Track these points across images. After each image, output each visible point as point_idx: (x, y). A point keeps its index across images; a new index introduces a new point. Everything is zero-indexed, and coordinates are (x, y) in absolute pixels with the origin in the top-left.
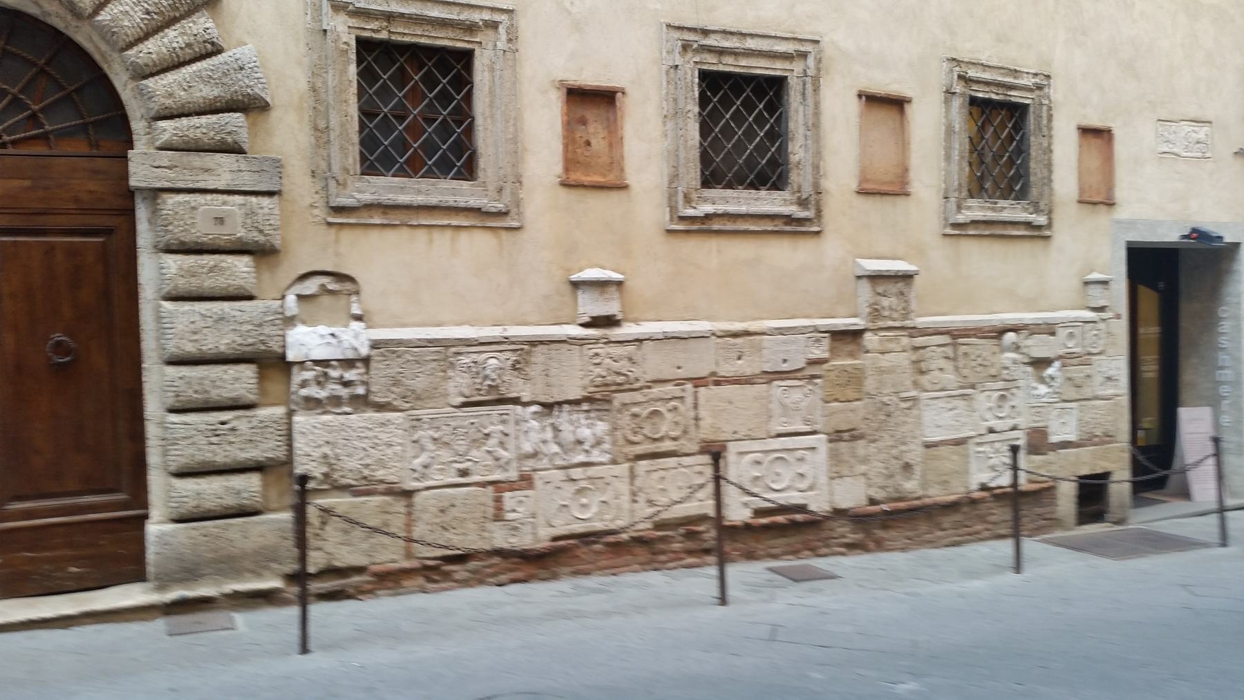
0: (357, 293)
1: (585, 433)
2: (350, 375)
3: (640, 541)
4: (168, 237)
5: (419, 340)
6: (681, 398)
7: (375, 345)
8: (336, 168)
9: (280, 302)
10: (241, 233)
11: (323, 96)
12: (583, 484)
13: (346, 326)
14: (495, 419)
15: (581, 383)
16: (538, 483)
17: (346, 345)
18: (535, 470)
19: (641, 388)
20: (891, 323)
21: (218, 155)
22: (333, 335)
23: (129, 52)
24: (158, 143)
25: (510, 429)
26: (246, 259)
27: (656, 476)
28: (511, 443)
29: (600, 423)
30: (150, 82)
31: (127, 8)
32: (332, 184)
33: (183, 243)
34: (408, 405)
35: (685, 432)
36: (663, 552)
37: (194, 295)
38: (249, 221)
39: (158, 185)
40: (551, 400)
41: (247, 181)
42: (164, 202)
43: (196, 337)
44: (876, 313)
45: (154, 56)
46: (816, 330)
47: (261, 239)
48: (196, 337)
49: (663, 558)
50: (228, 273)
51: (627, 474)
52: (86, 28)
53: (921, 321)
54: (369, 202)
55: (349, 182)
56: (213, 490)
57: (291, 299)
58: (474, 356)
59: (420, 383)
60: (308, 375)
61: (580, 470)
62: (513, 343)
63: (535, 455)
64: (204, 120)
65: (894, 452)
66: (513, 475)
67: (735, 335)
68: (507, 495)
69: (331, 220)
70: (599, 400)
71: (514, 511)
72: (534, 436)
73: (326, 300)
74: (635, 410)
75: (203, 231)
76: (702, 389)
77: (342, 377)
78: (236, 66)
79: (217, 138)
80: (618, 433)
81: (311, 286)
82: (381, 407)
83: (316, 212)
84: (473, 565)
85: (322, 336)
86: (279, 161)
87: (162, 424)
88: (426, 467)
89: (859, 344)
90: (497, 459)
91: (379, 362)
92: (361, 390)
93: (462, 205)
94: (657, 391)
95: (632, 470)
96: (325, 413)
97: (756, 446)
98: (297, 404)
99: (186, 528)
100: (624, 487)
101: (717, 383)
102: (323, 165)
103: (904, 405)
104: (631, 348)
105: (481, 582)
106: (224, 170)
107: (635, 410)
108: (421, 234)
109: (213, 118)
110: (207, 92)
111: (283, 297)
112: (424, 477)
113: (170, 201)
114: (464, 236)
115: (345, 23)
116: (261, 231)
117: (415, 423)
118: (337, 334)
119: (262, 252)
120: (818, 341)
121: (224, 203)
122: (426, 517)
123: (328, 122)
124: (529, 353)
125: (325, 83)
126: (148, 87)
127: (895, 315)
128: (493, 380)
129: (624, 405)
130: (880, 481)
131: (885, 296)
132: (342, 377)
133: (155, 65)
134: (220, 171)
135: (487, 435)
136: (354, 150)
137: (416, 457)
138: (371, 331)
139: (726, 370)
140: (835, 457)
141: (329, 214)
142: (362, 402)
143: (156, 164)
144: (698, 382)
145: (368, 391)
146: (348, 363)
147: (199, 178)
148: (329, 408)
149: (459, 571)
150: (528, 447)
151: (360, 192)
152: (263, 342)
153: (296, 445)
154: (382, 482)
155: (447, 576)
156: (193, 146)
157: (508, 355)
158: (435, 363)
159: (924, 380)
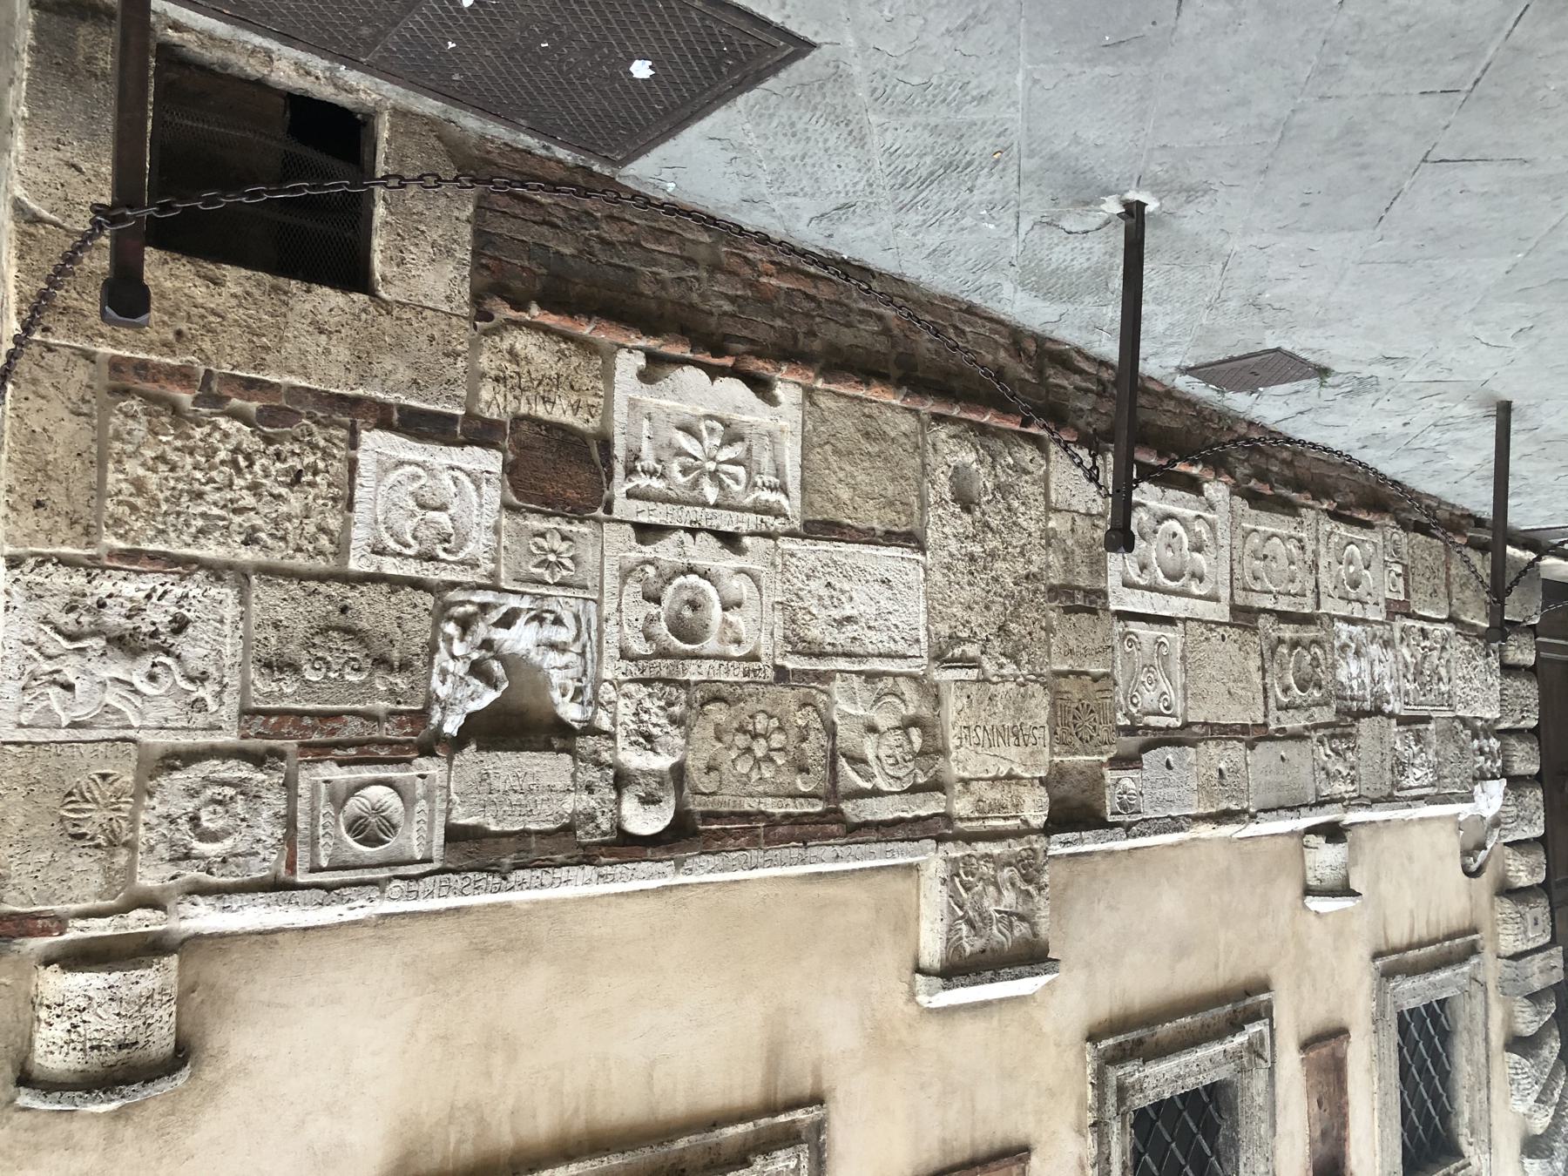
20: (996, 849)
44: (1029, 870)
65: (993, 543)
103: (972, 650)
127: (987, 869)
130: (1028, 488)
131: (1010, 914)
159: (914, 705)
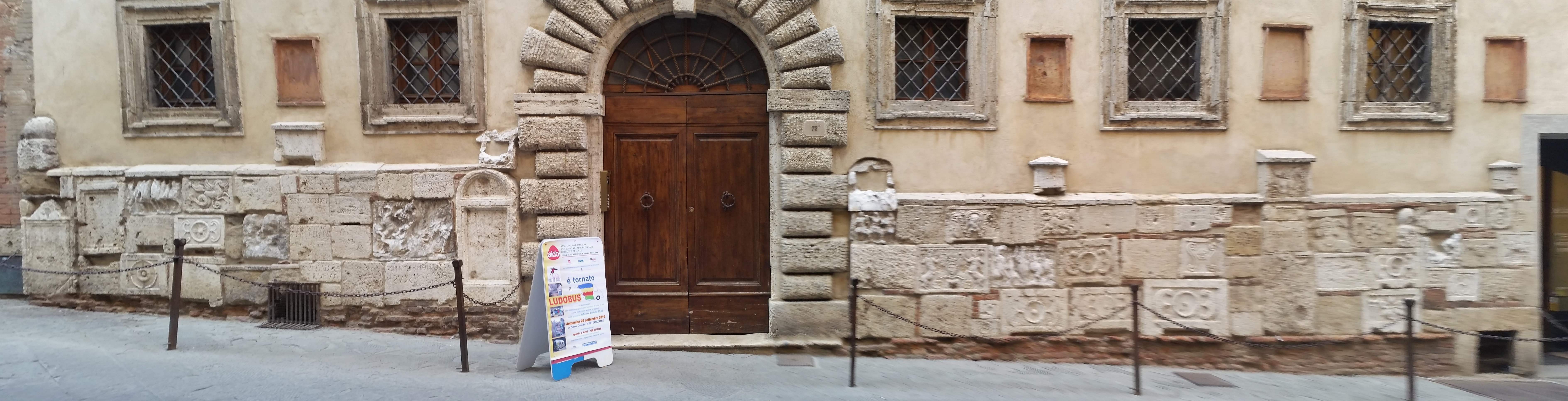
0: (891, 171)
1: (1037, 265)
2: (885, 221)
3: (1074, 342)
4: (787, 138)
5: (928, 201)
6: (1109, 246)
7: (901, 203)
8: (881, 96)
9: (846, 176)
10: (826, 135)
11: (875, 53)
12: (1034, 300)
13: (884, 191)
14: (975, 253)
15: (1034, 232)
16: (1003, 296)
17: (883, 202)
18: (1001, 288)
19: (1078, 238)
20: (1288, 199)
21: (815, 91)
22: (876, 196)
23: (770, 35)
24: (783, 85)
25: (985, 259)
26: (828, 150)
27: (1087, 298)
28: (985, 269)
29: (1047, 260)
30: (780, 51)
31: (770, 10)
32: (879, 105)
33: (795, 141)
34: (920, 241)
35: (1111, 270)
36: (1092, 352)
37: (799, 171)
38: (830, 128)
39: (783, 109)
40: (1014, 243)
41: (831, 105)
42: (786, 118)
43: (799, 195)
44: (1274, 190)
45: (783, 36)
46: (1221, 201)
47: (837, 138)
48: (799, 195)
49: (1091, 355)
50: (818, 158)
51: (1066, 295)
52: (748, 23)
53: (1316, 198)
54: (900, 116)
55: (888, 104)
56: (805, 284)
57: (852, 174)
58: (963, 212)
59: (927, 228)
60: (861, 219)
61: (1032, 290)
62: (989, 204)
63: (1001, 278)
64: (808, 71)
65: (1289, 297)
66: (986, 289)
67: (1153, 204)
68: (981, 302)
69: (877, 127)
70: (1047, 244)
71: (986, 313)
72: (1001, 266)
73: (873, 175)
74: (1074, 252)
75: (806, 134)
76: (1125, 241)
77: (880, 222)
78: (826, 39)
79: (815, 81)
80: (1061, 268)
81: (864, 167)
82: (903, 241)
83: (869, 122)
84: (957, 345)
85: (870, 197)
86: (848, 93)
87: (779, 244)
88: (929, 280)
89: (1258, 214)
90: (976, 279)
91: (903, 213)
92: (891, 230)
93: (958, 116)
94: (1090, 240)
95: (1070, 293)
96: (869, 243)
97: (1167, 283)
98: (853, 236)
99: (790, 305)
100: (1064, 304)
101: (1137, 237)
102: (874, 94)
104: (1071, 211)
105: (963, 357)
106: (818, 100)
107: (1074, 252)
108: (931, 135)
109: (813, 69)
110: (810, 55)
111: (848, 173)
112: (928, 286)
113: (789, 118)
114: (958, 136)
115: (889, 8)
116: (837, 134)
117: (923, 252)
118: (878, 195)
119: (837, 146)
120: (1222, 210)
121: (818, 118)
122: (928, 311)
123: (877, 69)
124: (999, 211)
125: (876, 45)
126: (779, 53)
127: (1293, 192)
128: (975, 228)
129: (1066, 248)
130: (1276, 318)
131: (1283, 178)
132: (880, 222)
133: (783, 41)
134: (816, 100)
135: (970, 263)
136: (892, 85)
137: (923, 273)
138: (898, 194)
139: (1144, 228)
140: (1234, 297)
141: (876, 124)
142: (892, 237)
143: (782, 97)
144: (1122, 236)
145: (896, 231)
146: (884, 214)
147: (805, 104)
148: (872, 240)
149: (949, 348)
150: (996, 272)
151: (894, 110)
152: (836, 199)
153: (852, 261)
154: (902, 287)
155: (941, 350)
156: (802, 86)
157: (985, 212)
158: (937, 215)
159: (1319, 243)
